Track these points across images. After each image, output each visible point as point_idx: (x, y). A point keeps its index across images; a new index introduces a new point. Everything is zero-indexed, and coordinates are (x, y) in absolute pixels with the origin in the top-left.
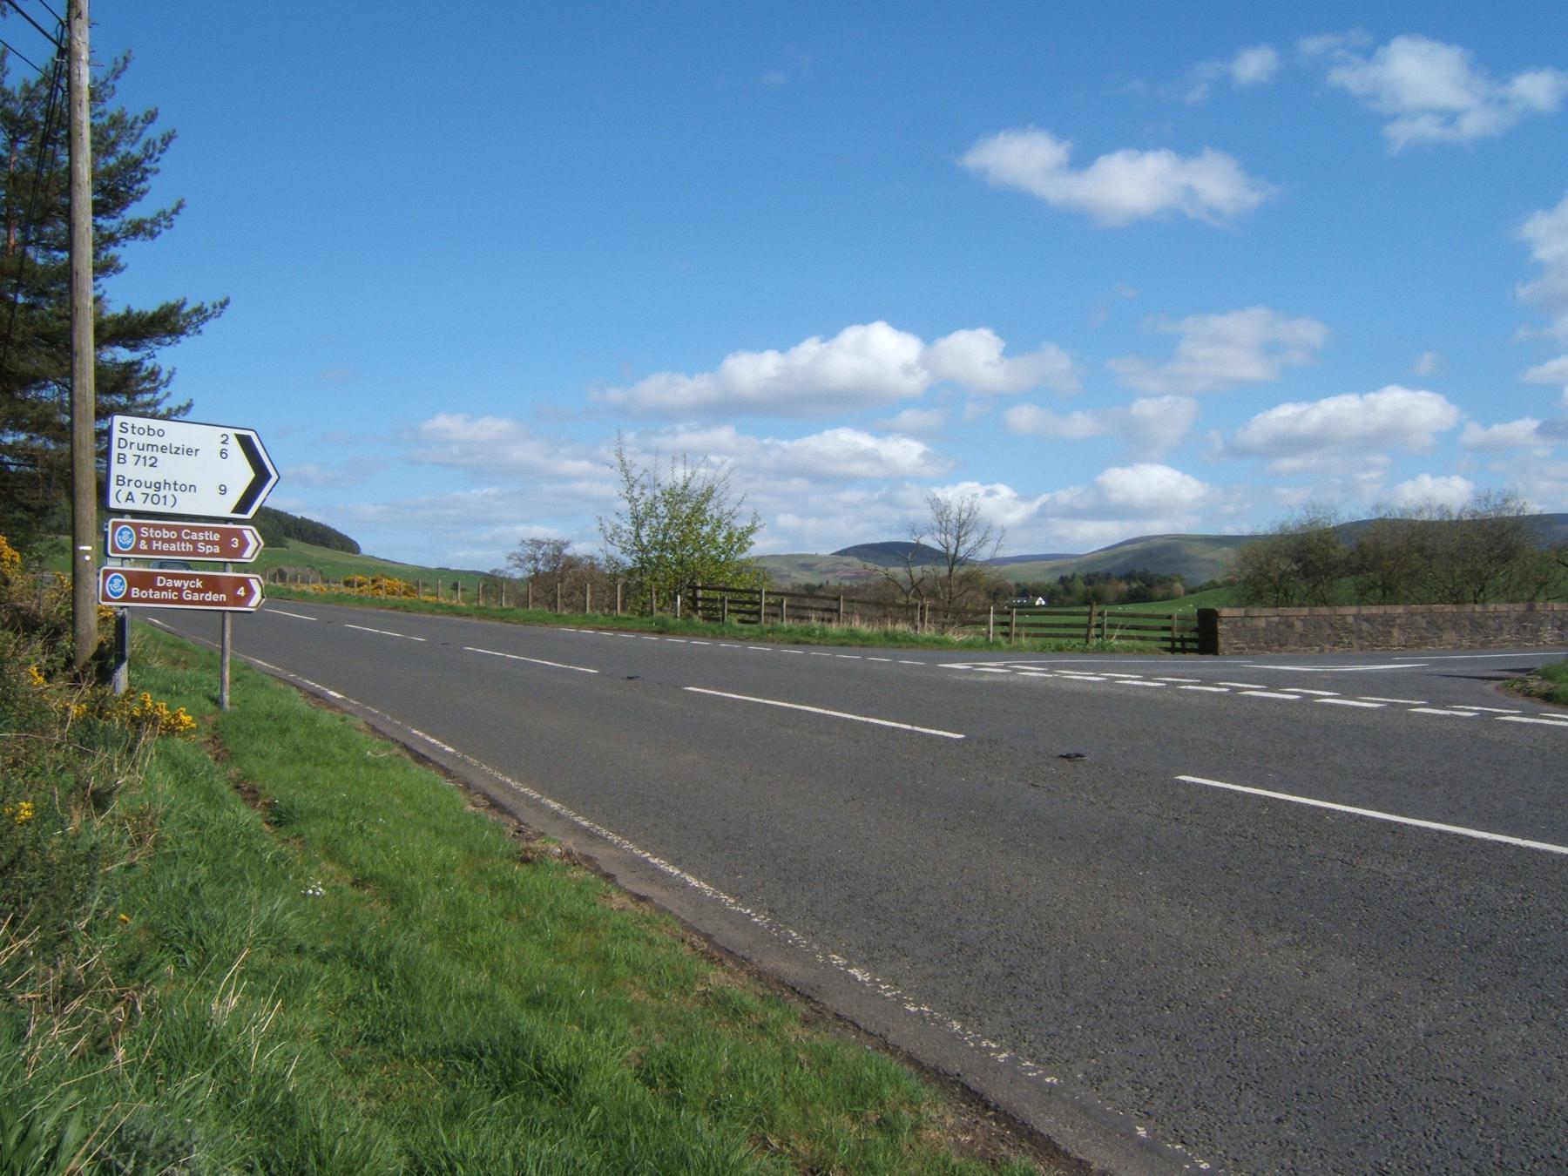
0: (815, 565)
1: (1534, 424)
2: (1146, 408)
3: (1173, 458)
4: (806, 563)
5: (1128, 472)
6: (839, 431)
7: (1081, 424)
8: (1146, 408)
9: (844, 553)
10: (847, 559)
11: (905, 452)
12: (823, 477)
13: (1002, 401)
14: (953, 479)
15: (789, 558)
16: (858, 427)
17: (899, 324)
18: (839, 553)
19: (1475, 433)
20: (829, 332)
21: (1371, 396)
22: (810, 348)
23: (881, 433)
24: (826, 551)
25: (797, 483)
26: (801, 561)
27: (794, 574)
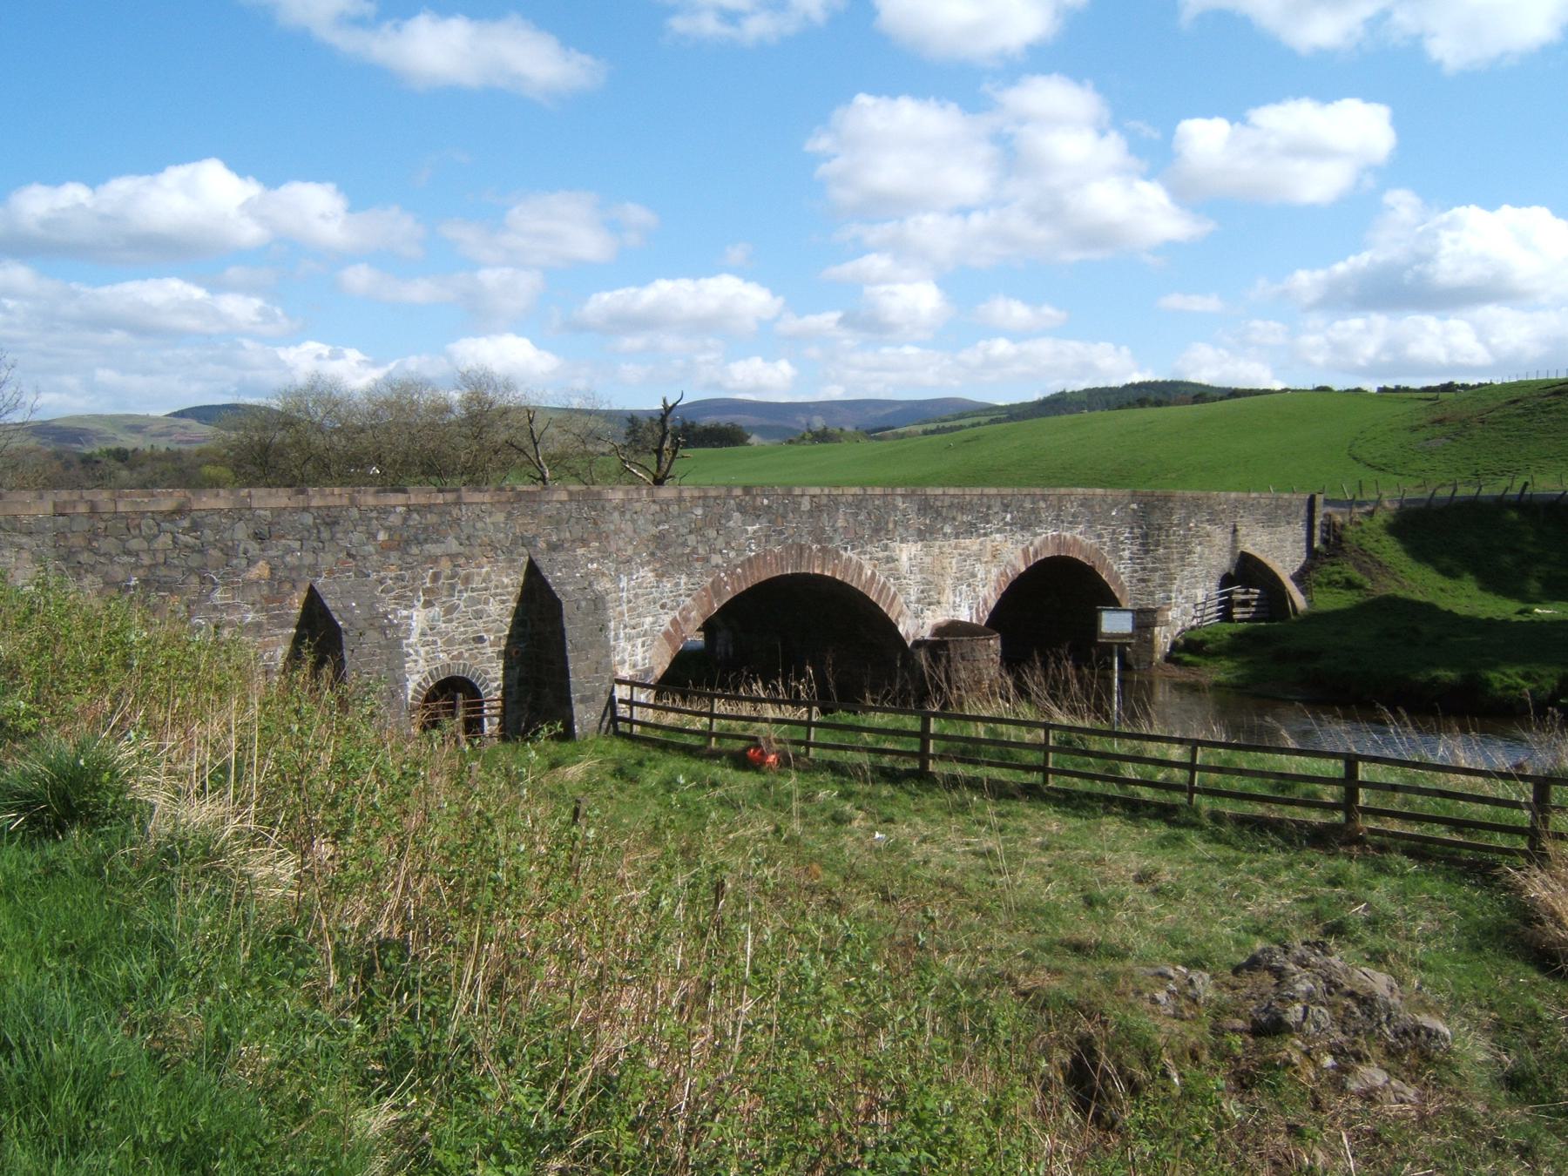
0: (146, 427)
1: (834, 316)
2: (490, 277)
3: (518, 327)
4: (136, 426)
5: (483, 341)
6: (166, 280)
7: (420, 291)
8: (490, 277)
9: (181, 414)
10: (184, 422)
11: (240, 308)
12: (143, 328)
13: (342, 259)
14: (294, 339)
15: (113, 420)
16: (188, 277)
17: (239, 167)
18: (175, 415)
19: (792, 324)
20: (151, 164)
21: (702, 281)
22: (121, 187)
23: (217, 286)
24: (160, 412)
25: (117, 336)
26: (130, 422)
27: (120, 436)
